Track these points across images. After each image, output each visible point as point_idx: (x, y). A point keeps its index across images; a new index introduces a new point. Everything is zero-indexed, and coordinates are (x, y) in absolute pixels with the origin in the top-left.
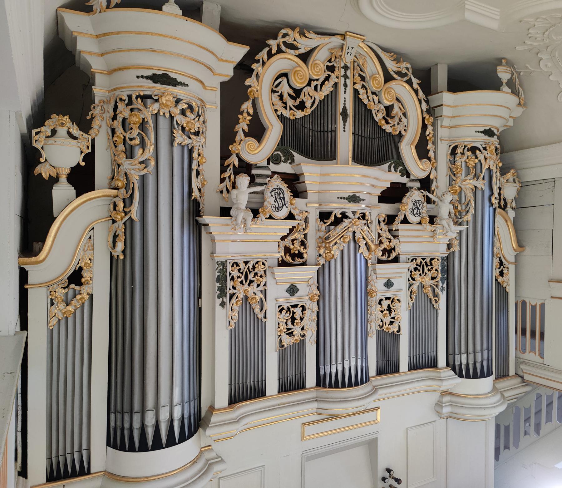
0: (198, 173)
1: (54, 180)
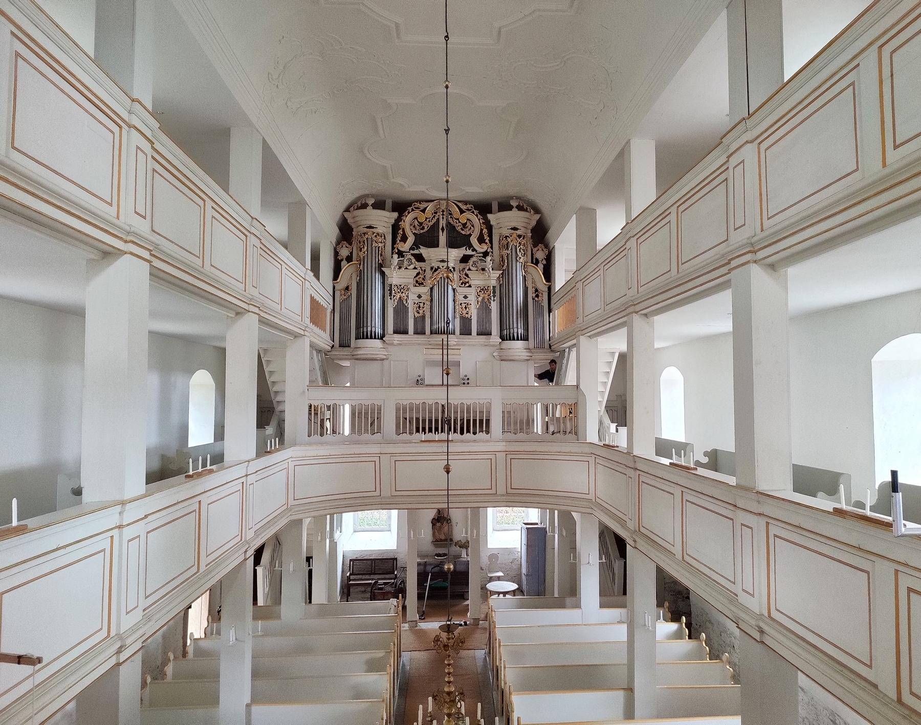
1: (342, 260)
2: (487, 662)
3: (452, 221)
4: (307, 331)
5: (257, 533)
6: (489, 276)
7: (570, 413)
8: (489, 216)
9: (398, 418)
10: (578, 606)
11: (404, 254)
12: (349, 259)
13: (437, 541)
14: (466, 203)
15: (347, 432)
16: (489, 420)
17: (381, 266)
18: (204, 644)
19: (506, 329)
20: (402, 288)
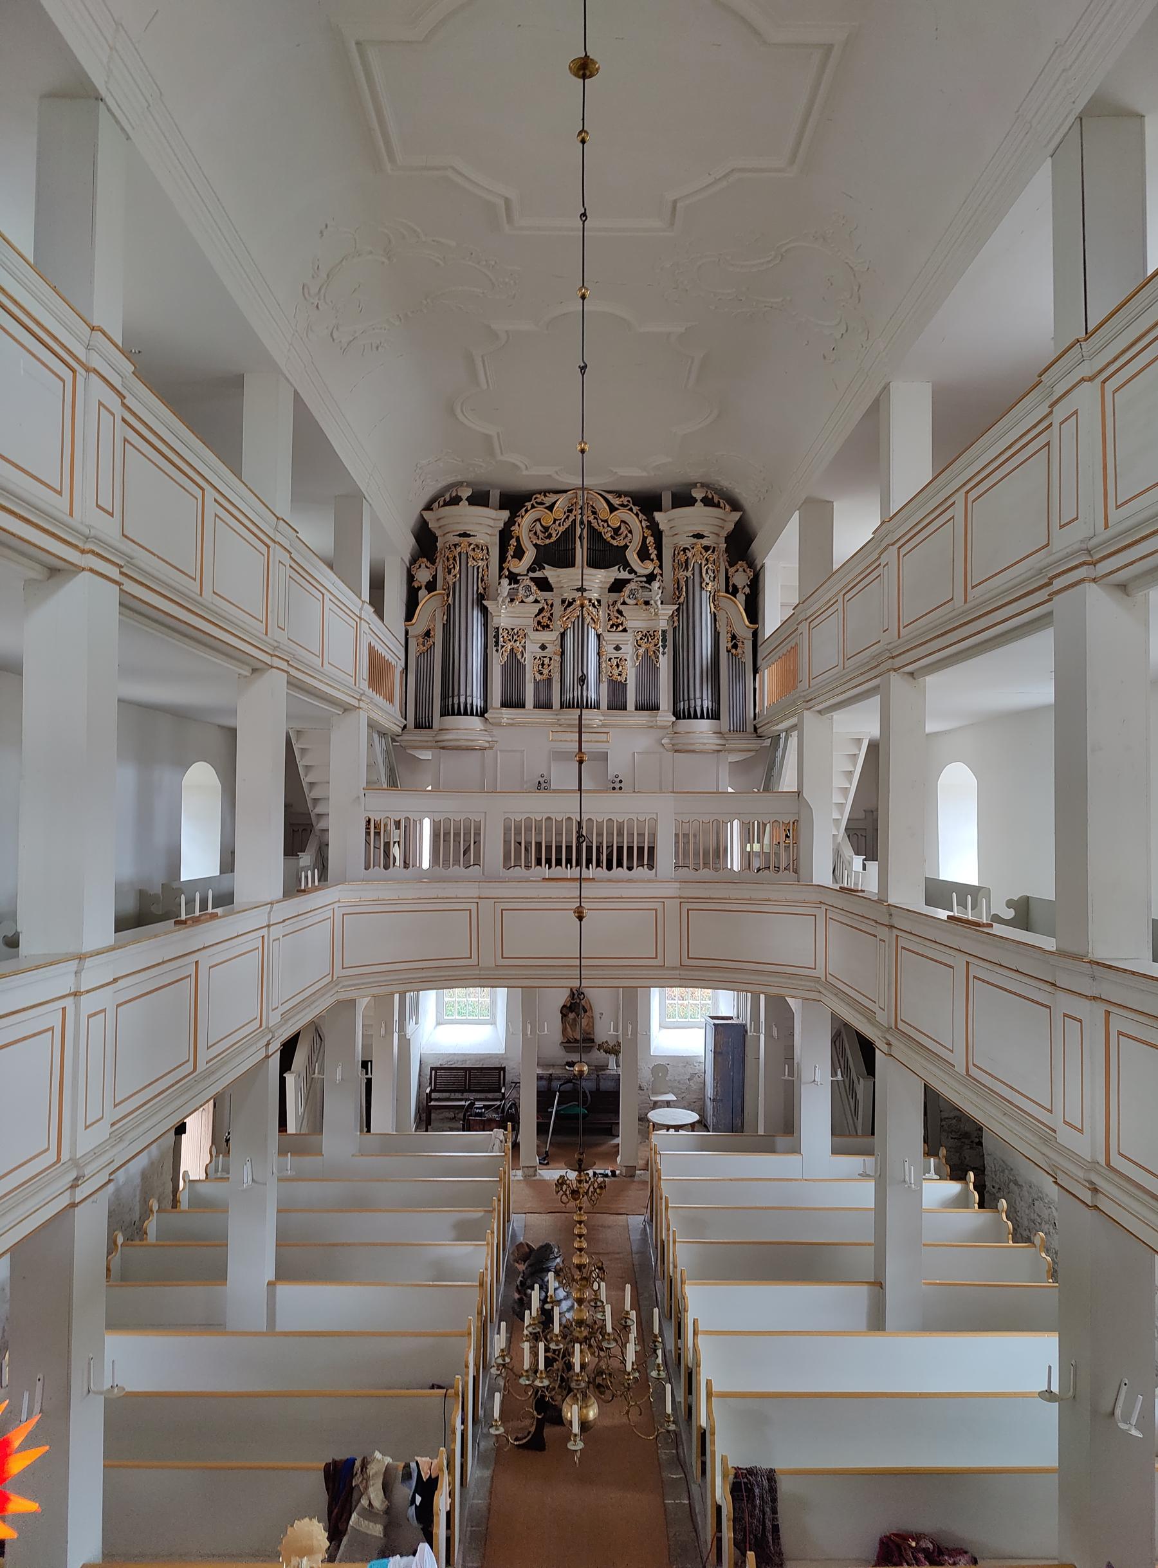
0: (482, 580)
1: (420, 588)
2: (646, 1235)
3: (596, 524)
4: (363, 701)
5: (285, 1017)
6: (656, 614)
7: (787, 836)
8: (658, 516)
9: (507, 842)
10: (796, 1150)
11: (518, 578)
12: (431, 586)
13: (569, 1042)
14: (619, 494)
15: (426, 865)
16: (654, 847)
17: (481, 597)
18: (203, 1189)
19: (684, 700)
20: (515, 634)
